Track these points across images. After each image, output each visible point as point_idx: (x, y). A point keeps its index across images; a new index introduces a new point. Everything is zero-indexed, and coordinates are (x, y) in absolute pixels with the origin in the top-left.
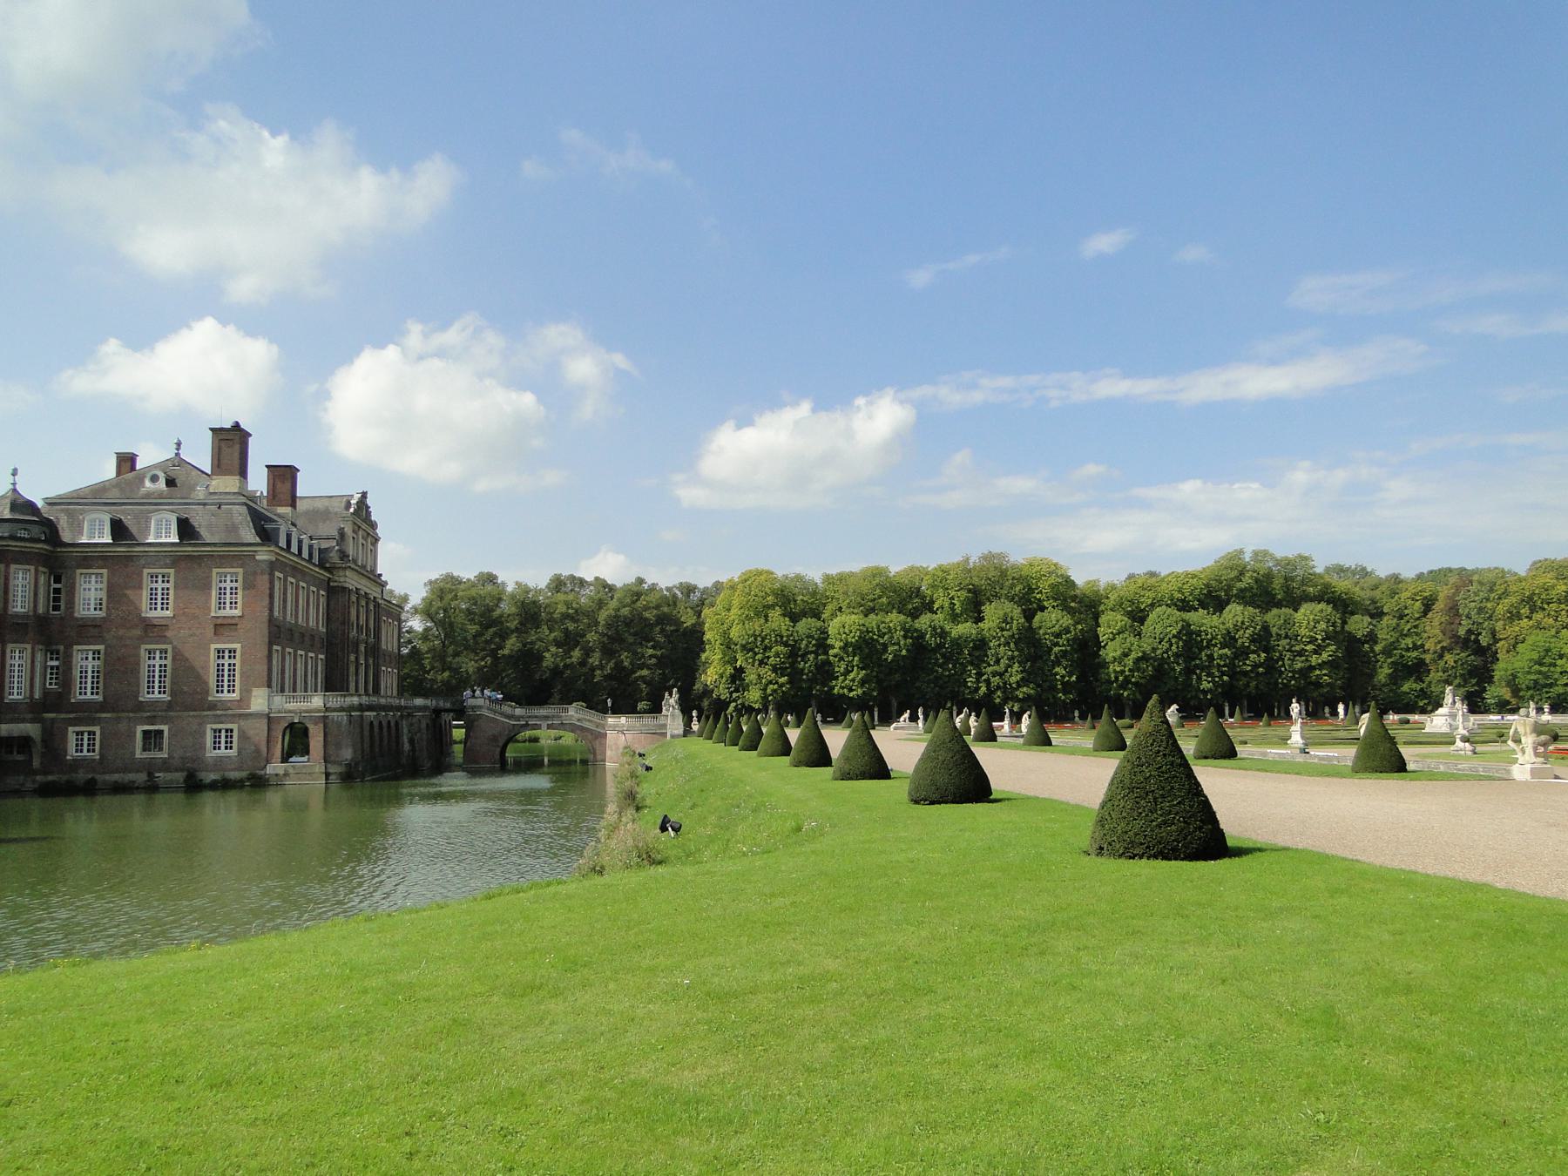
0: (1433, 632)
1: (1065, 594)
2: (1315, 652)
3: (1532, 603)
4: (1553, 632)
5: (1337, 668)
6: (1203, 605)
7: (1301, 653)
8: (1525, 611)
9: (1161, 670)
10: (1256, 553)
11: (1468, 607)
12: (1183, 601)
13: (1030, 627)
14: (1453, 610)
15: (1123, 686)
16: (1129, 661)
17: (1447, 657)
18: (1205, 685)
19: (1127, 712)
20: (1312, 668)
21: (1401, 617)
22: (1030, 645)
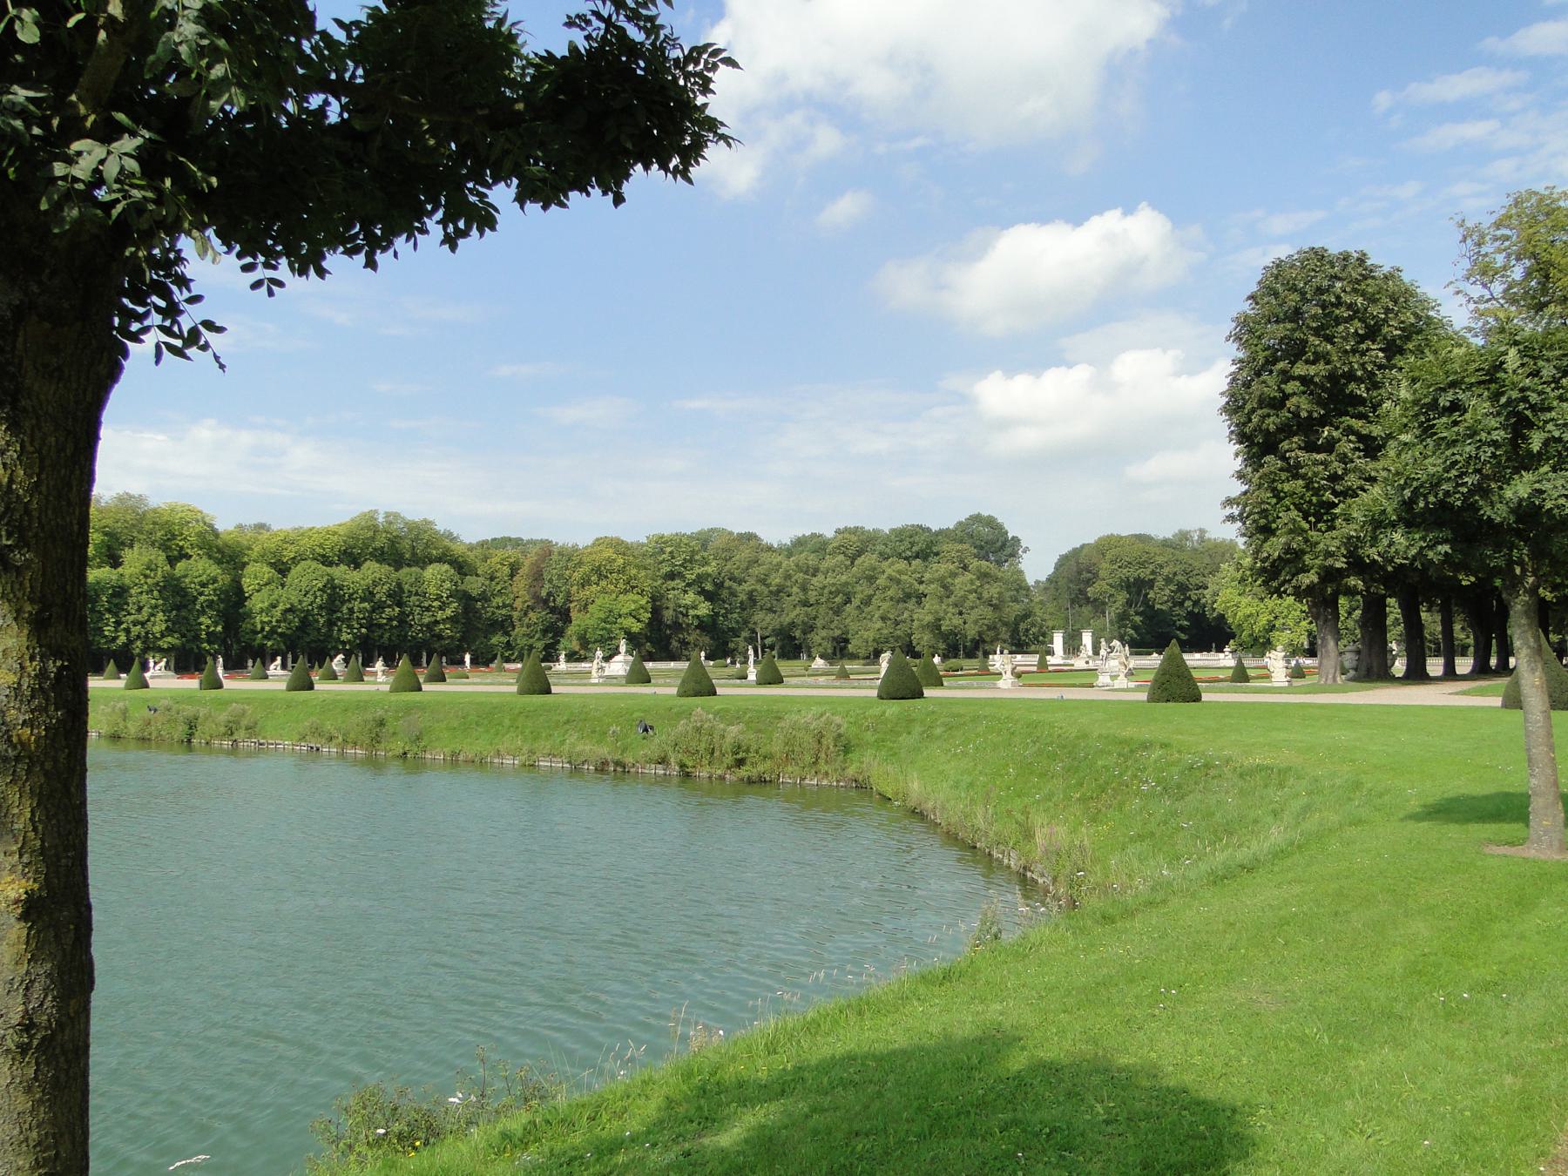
2: (440, 608)
3: (600, 573)
7: (428, 609)
10: (387, 515)
11: (551, 573)
14: (538, 576)
16: (277, 613)
17: (531, 614)
18: (345, 637)
20: (437, 622)
21: (492, 579)
22: (176, 596)
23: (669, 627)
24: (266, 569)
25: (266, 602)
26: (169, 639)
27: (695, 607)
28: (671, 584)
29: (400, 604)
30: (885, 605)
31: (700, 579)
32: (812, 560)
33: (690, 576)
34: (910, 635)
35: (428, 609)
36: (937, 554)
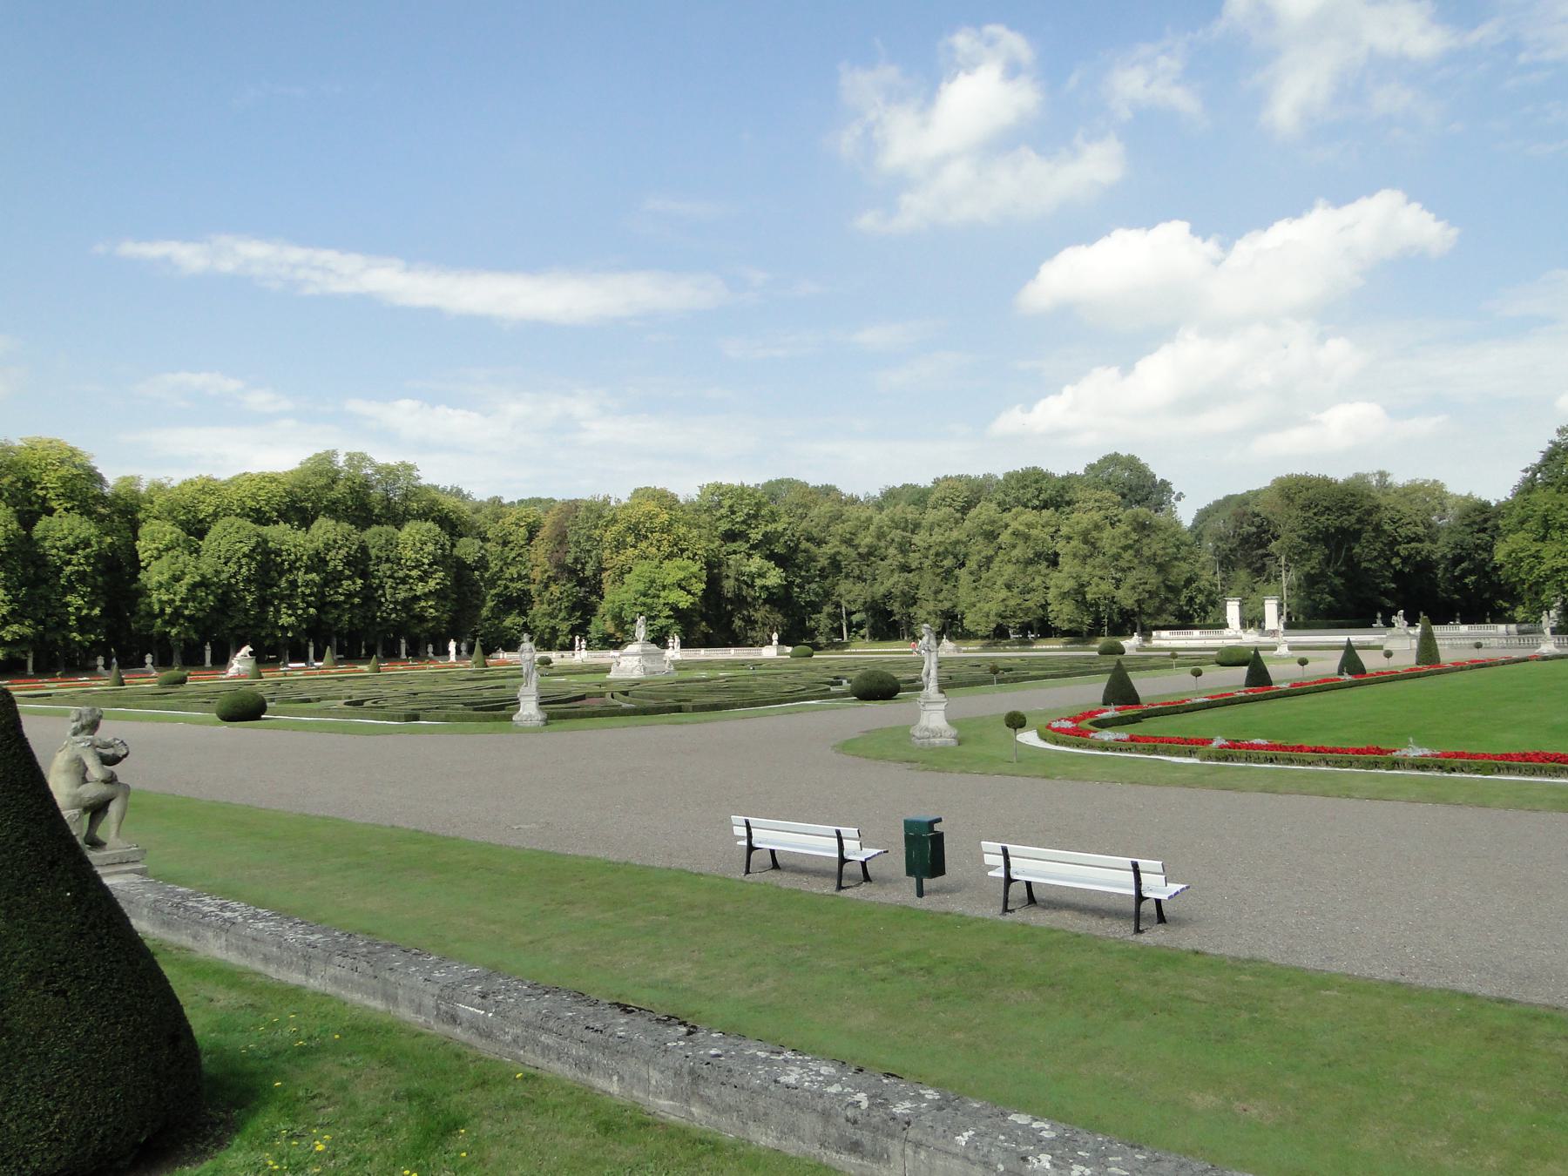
0: (539, 560)
1: (84, 492)
3: (637, 532)
4: (656, 562)
5: (445, 598)
6: (284, 516)
7: (403, 581)
8: (630, 539)
9: (226, 599)
10: (351, 457)
12: (258, 511)
13: (29, 537)
14: (561, 539)
15: (171, 622)
16: (182, 588)
17: (553, 588)
18: (285, 620)
19: (177, 658)
20: (416, 599)
21: (505, 544)
23: (730, 601)
24: (168, 527)
25: (163, 573)
26: (15, 628)
27: (762, 575)
28: (733, 546)
29: (364, 575)
30: (1009, 570)
31: (768, 539)
32: (912, 513)
33: (756, 535)
34: (1044, 606)
35: (403, 581)
36: (1069, 503)
